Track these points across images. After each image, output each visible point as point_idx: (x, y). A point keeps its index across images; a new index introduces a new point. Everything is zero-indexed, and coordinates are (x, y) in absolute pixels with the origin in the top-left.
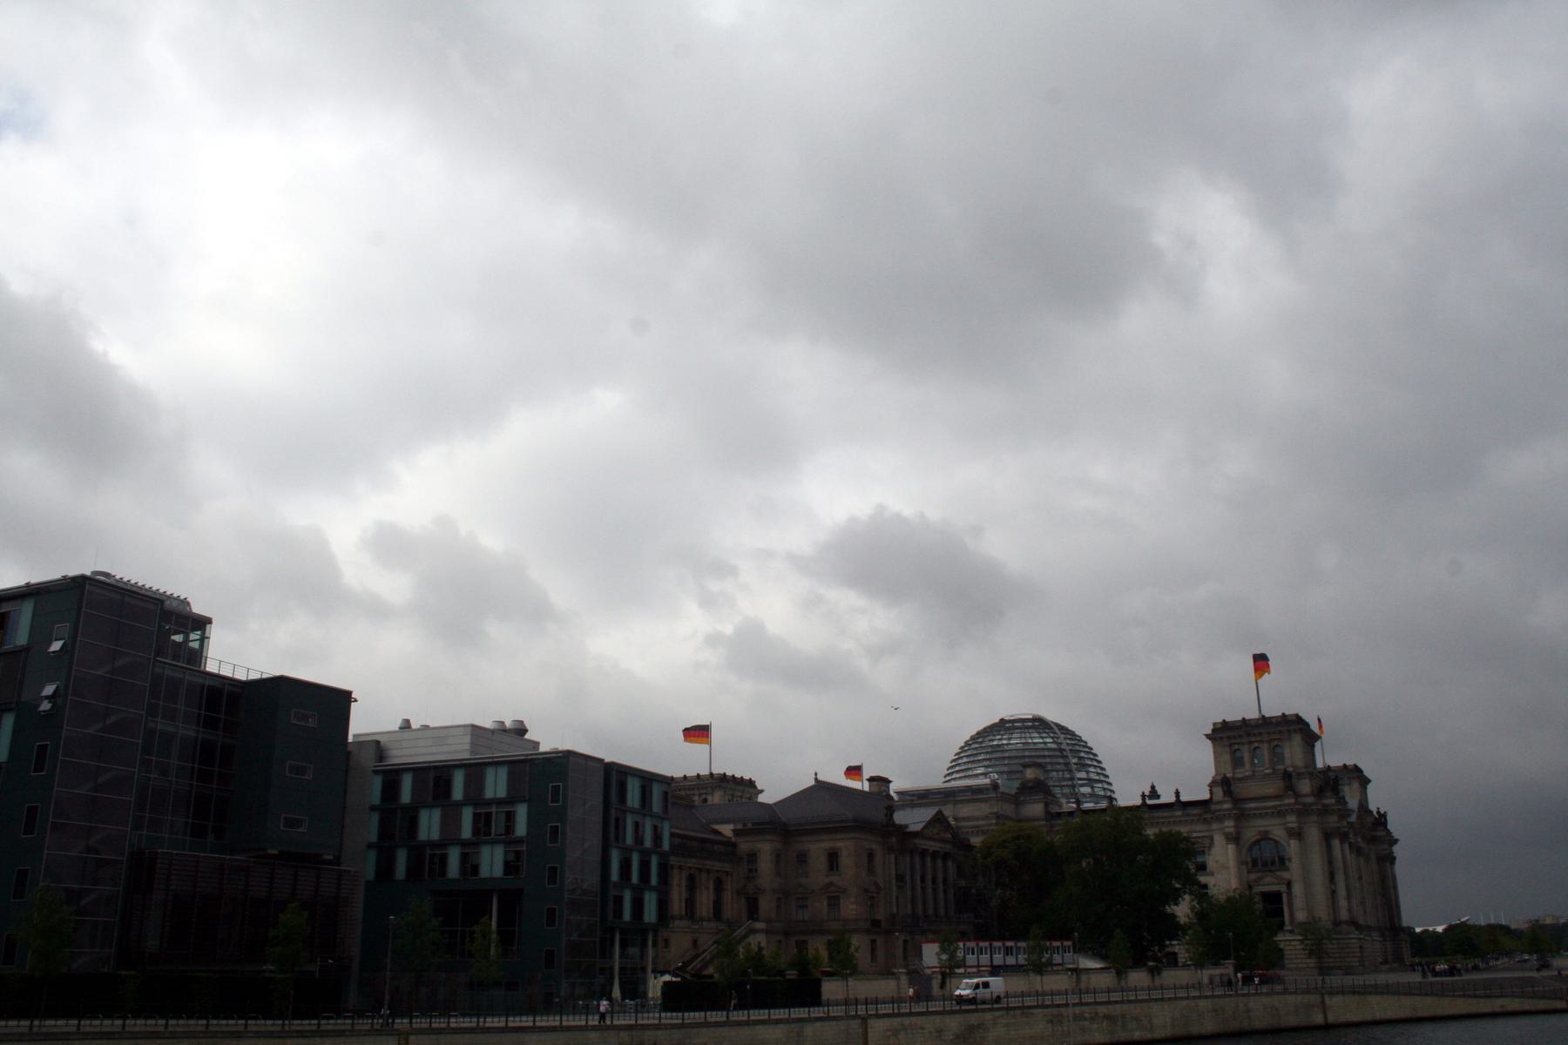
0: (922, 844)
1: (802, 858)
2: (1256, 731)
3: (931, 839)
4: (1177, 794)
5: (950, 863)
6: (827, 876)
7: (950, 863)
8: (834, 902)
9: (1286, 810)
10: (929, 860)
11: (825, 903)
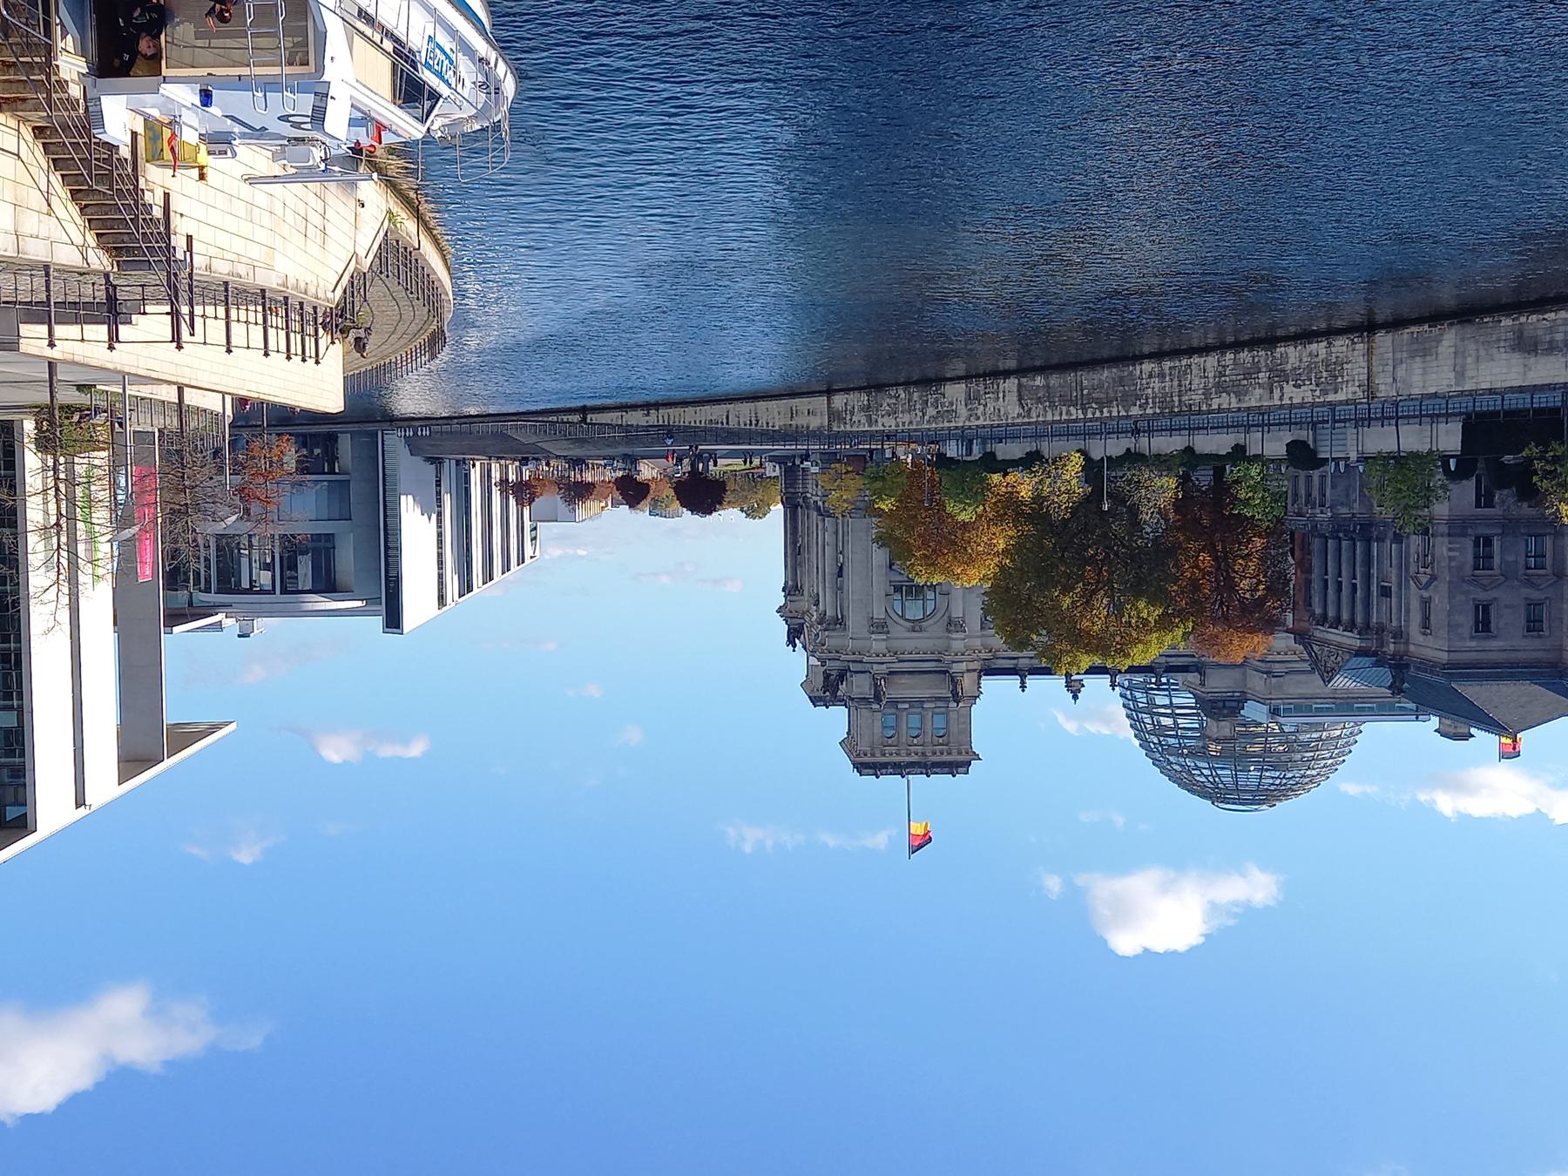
0: (1352, 640)
1: (1534, 624)
2: (914, 758)
3: (1339, 645)
4: (1023, 687)
5: (1318, 611)
6: (1495, 599)
7: (1318, 611)
8: (1483, 560)
9: (884, 656)
10: (1345, 616)
11: (1497, 560)
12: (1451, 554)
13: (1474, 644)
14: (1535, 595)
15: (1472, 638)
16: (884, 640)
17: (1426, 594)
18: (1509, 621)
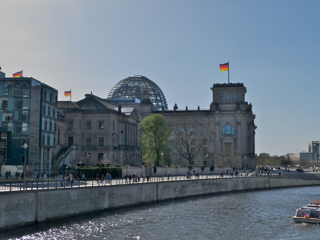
1: (89, 124)
11: (98, 140)
12: (109, 142)
13: (104, 119)
14: (89, 131)
15: (104, 120)
16: (238, 120)
17: (114, 131)
18: (95, 125)
